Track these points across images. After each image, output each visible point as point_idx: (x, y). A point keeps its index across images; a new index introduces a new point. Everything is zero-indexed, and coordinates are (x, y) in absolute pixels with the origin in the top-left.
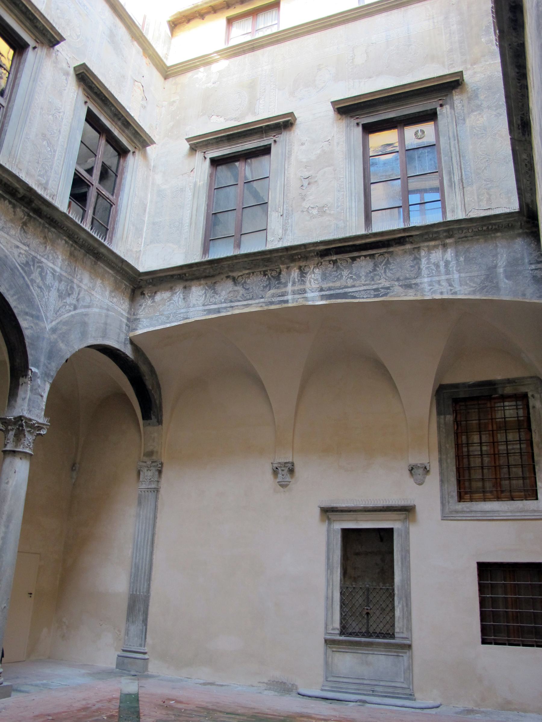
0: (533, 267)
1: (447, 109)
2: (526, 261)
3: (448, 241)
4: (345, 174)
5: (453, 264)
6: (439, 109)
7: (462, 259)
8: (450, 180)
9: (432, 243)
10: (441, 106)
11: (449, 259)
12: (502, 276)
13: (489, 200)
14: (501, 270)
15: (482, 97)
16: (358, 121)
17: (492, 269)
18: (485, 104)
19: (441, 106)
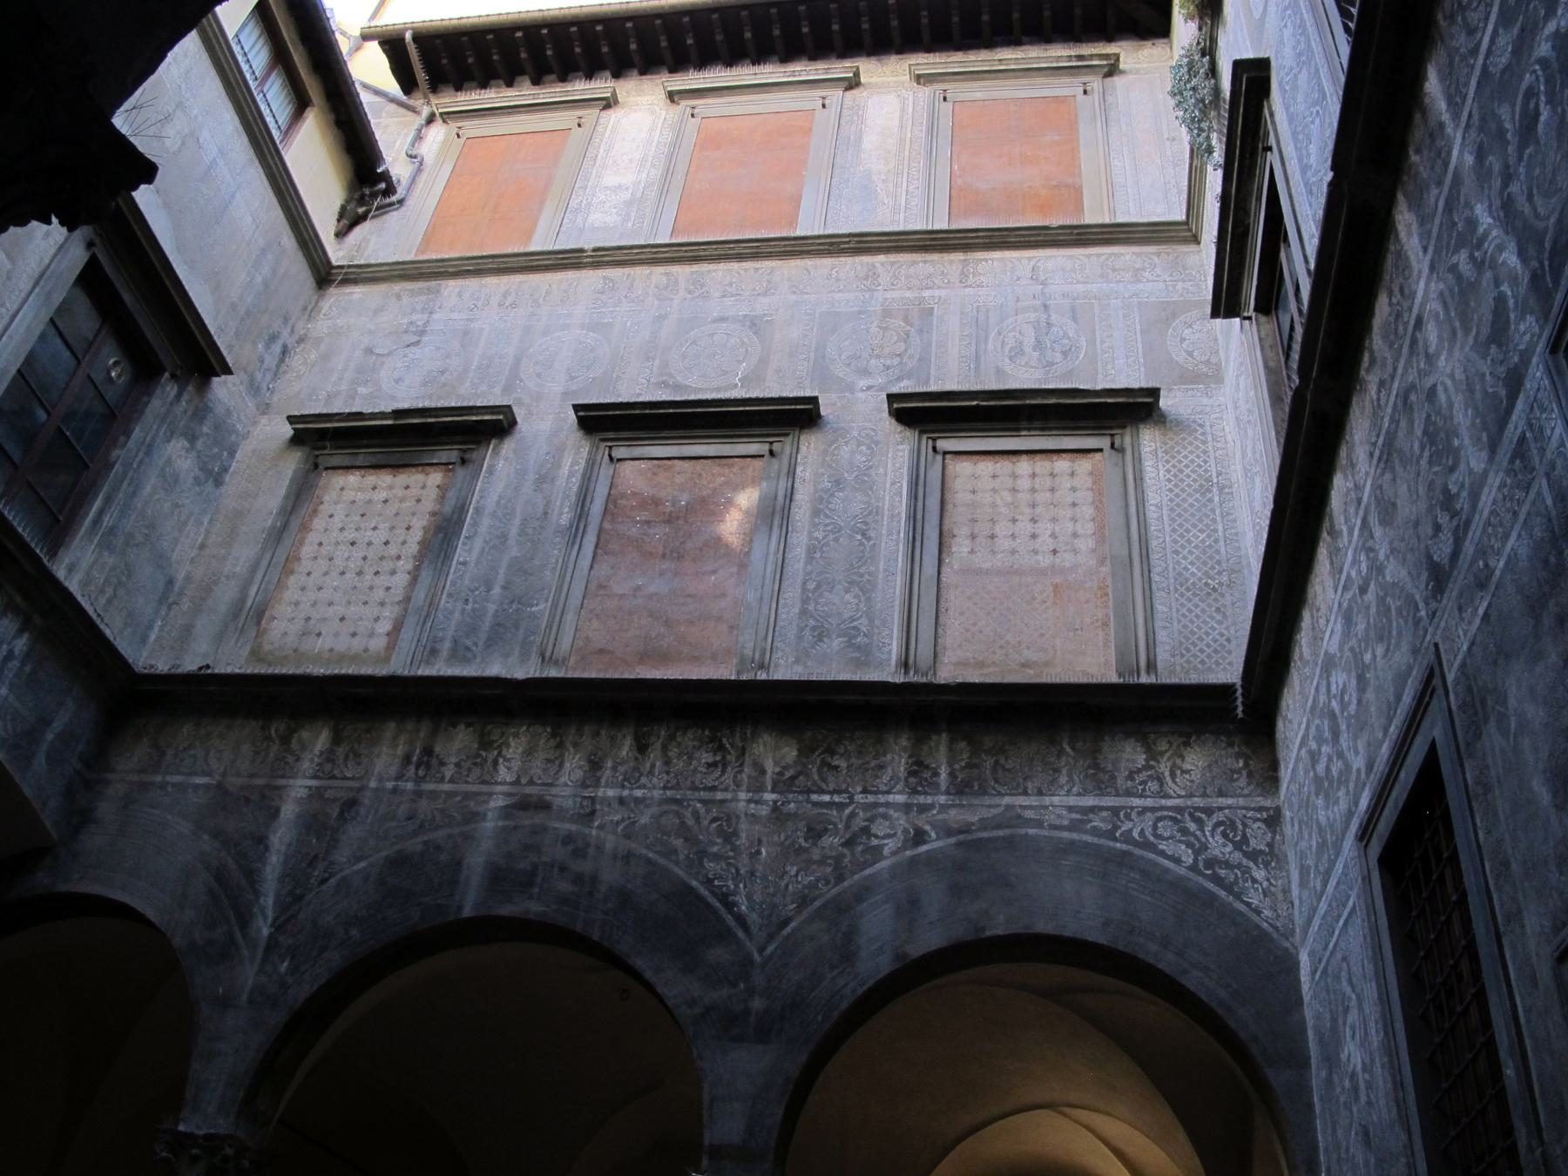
0: (79, 766)
1: (171, 389)
2: (80, 748)
3: (37, 620)
4: (15, 307)
5: (15, 664)
6: (167, 375)
7: (27, 669)
8: (101, 512)
9: (19, 599)
10: (173, 376)
11: (17, 651)
12: (44, 747)
13: (109, 602)
14: (50, 736)
15: (205, 429)
16: (97, 241)
17: (46, 722)
18: (199, 444)
19: (173, 376)
